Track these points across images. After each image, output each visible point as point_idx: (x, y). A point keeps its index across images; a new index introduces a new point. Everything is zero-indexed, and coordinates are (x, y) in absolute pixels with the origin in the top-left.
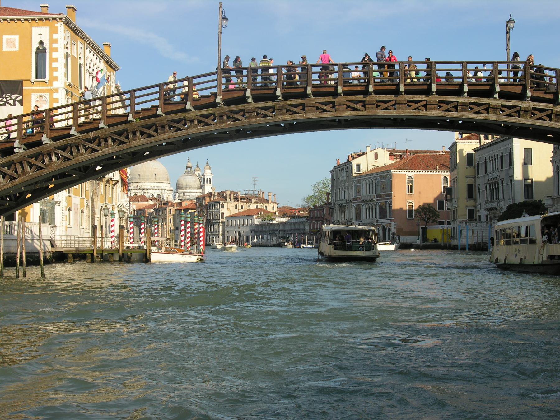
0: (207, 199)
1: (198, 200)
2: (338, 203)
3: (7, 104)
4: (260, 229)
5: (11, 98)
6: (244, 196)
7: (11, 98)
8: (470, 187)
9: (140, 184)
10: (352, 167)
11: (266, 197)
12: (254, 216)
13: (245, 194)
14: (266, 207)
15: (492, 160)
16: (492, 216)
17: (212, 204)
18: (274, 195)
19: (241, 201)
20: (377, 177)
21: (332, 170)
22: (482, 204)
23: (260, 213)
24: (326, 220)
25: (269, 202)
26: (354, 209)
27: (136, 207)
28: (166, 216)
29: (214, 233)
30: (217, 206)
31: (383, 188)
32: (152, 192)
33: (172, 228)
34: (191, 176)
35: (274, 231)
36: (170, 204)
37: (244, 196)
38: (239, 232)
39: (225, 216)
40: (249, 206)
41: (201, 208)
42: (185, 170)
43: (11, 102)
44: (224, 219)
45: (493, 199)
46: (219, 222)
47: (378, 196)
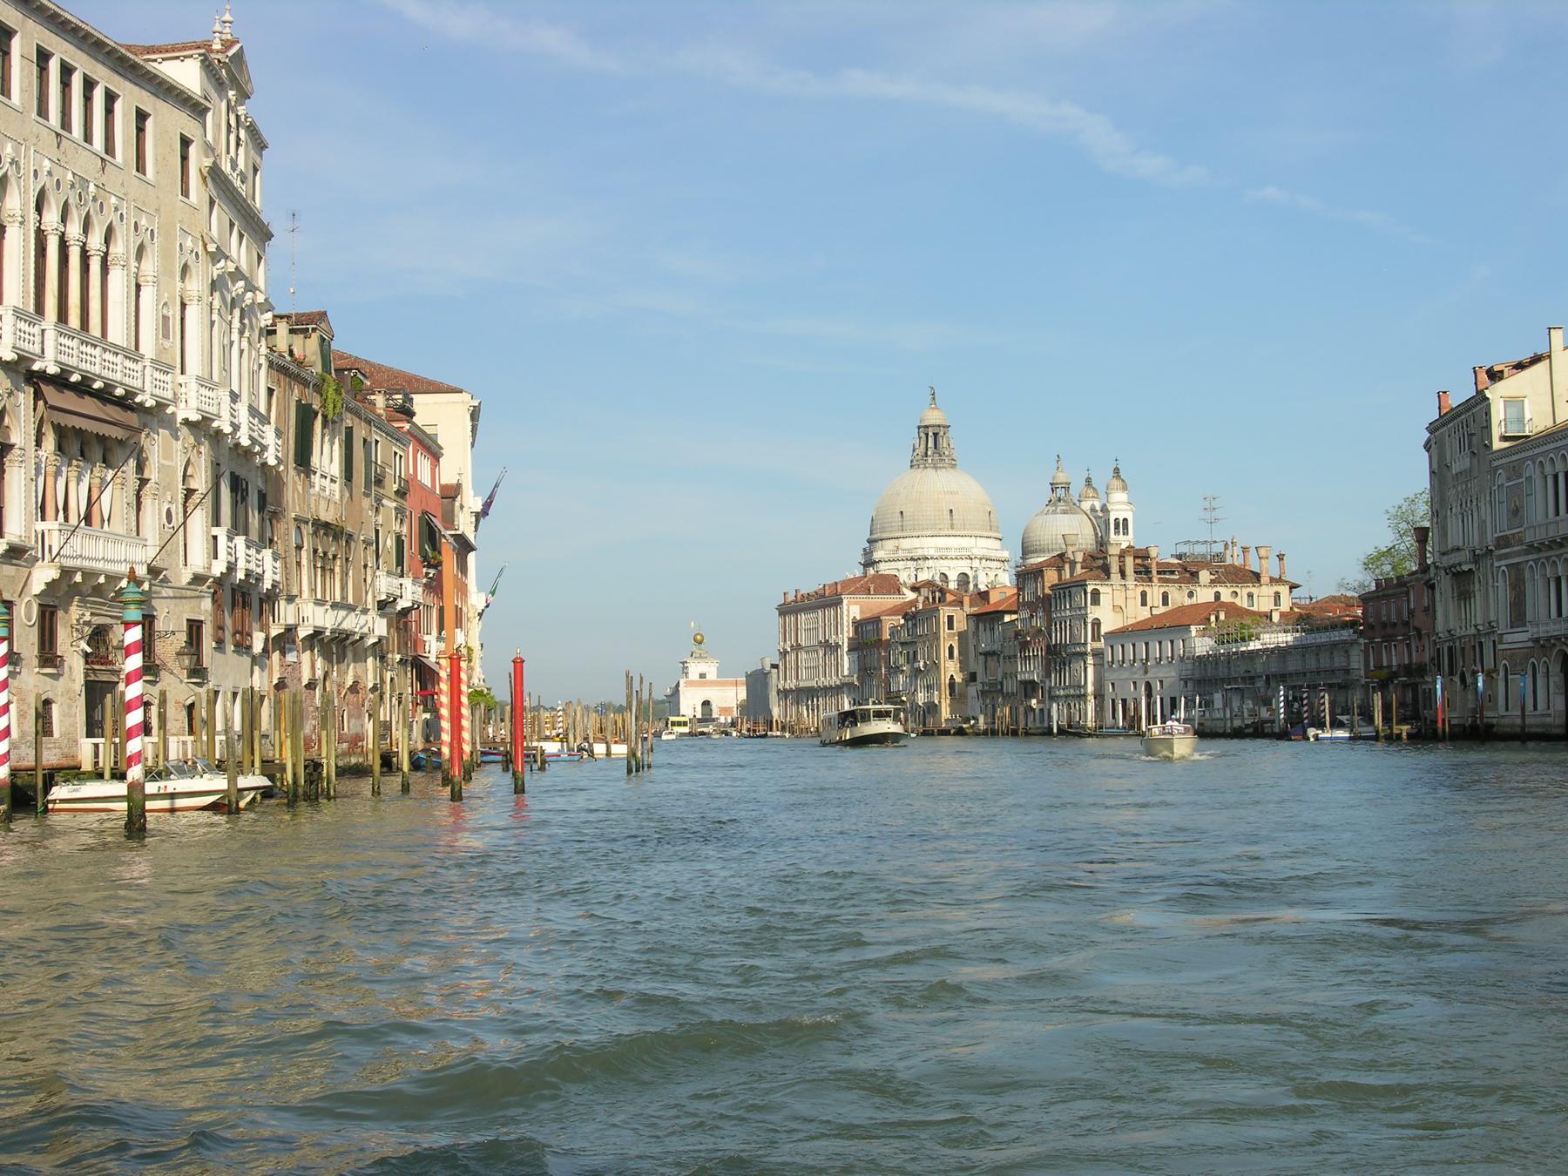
0: (1051, 577)
1: (1024, 580)
2: (1447, 561)
4: (1210, 672)
6: (1177, 561)
9: (905, 544)
10: (1488, 414)
12: (1193, 628)
13: (1179, 557)
14: (1250, 596)
17: (1065, 590)
18: (1281, 557)
19: (1160, 580)
21: (1429, 441)
23: (1213, 618)
25: (1264, 579)
26: (1500, 583)
27: (861, 612)
28: (936, 636)
29: (1072, 692)
30: (1079, 599)
32: (942, 566)
33: (958, 679)
34: (1065, 512)
35: (1252, 679)
36: (949, 598)
37: (1177, 561)
38: (1148, 686)
39: (1102, 633)
40: (1191, 595)
41: (1032, 607)
42: (1049, 494)
44: (1101, 644)
46: (1085, 654)
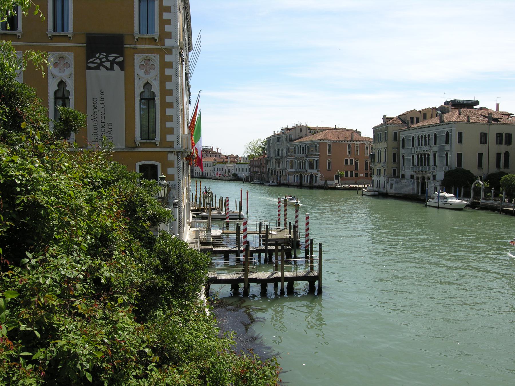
2: (275, 158)
3: (101, 67)
5: (107, 58)
7: (107, 58)
8: (395, 154)
11: (215, 150)
15: (422, 138)
16: (420, 176)
20: (306, 144)
22: (406, 167)
24: (263, 167)
26: (288, 162)
31: (312, 151)
43: (108, 64)
45: (421, 165)
47: (307, 156)
